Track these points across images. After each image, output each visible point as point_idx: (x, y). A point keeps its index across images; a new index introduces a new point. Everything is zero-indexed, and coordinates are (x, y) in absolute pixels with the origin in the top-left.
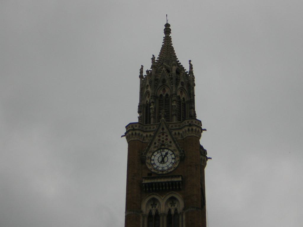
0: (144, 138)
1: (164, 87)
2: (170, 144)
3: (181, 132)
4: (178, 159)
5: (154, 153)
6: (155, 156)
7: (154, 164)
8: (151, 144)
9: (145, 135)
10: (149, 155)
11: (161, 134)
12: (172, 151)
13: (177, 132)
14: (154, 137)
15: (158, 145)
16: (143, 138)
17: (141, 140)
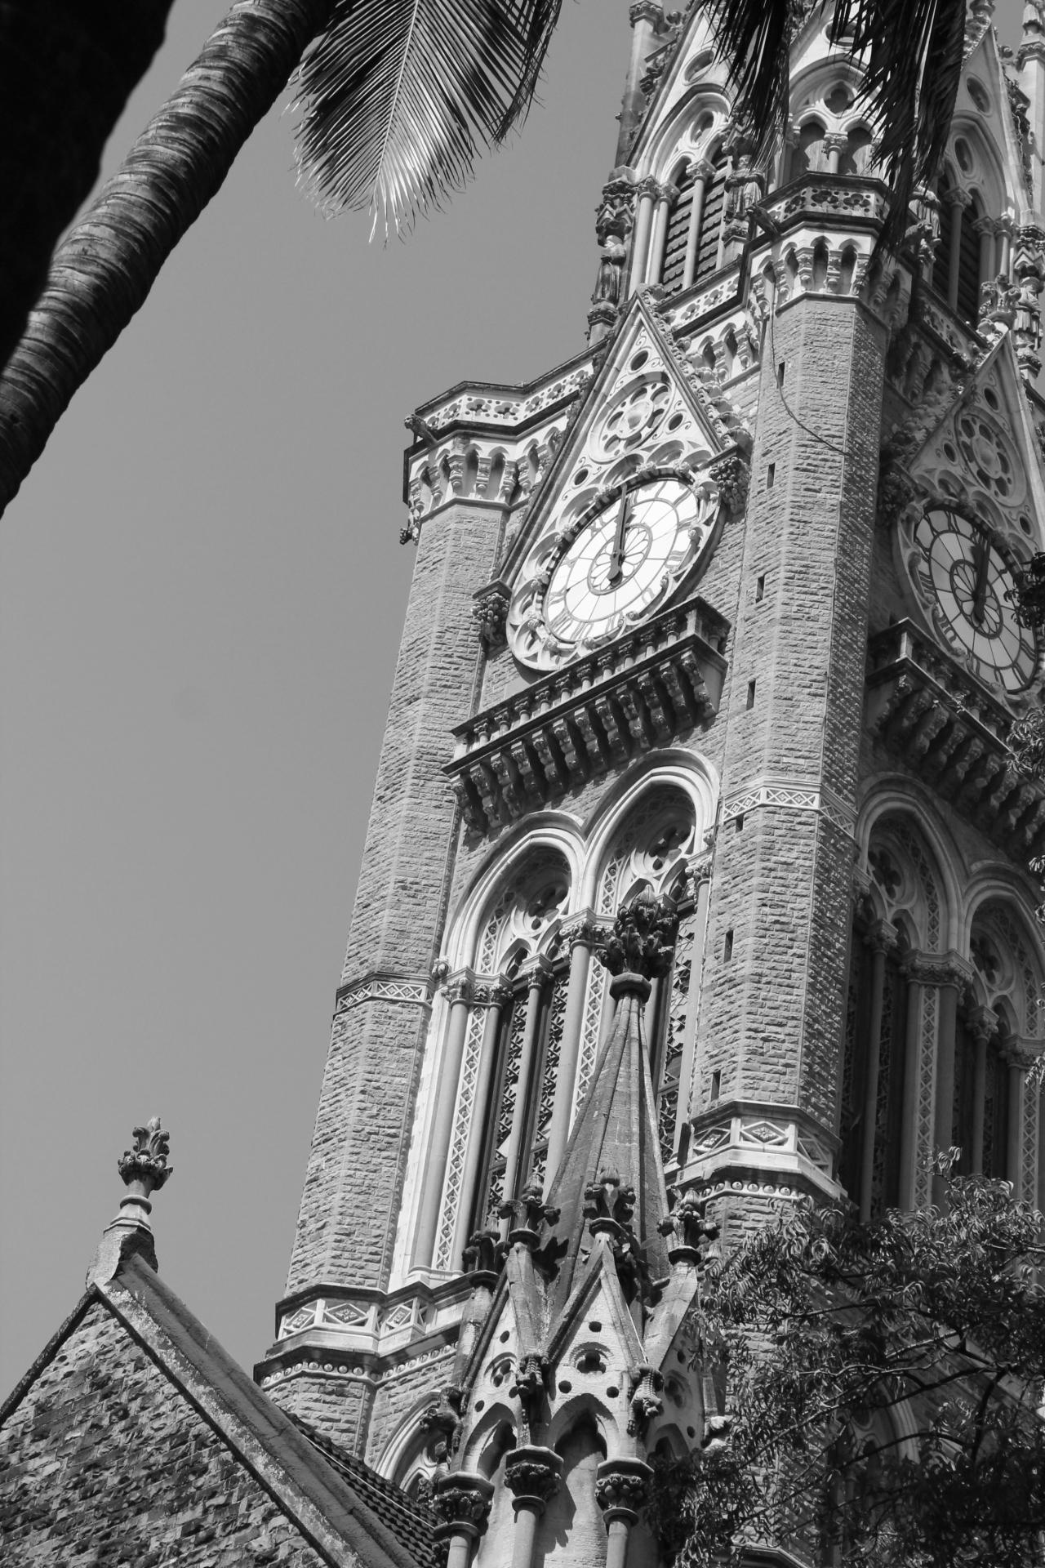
0: (516, 475)
1: (703, 103)
2: (664, 436)
3: (739, 319)
4: (713, 508)
5: (566, 545)
6: (573, 563)
7: (566, 616)
8: (547, 491)
9: (515, 452)
10: (531, 570)
11: (628, 400)
12: (685, 479)
13: (716, 333)
14: (567, 442)
15: (598, 480)
16: (506, 478)
17: (500, 500)
